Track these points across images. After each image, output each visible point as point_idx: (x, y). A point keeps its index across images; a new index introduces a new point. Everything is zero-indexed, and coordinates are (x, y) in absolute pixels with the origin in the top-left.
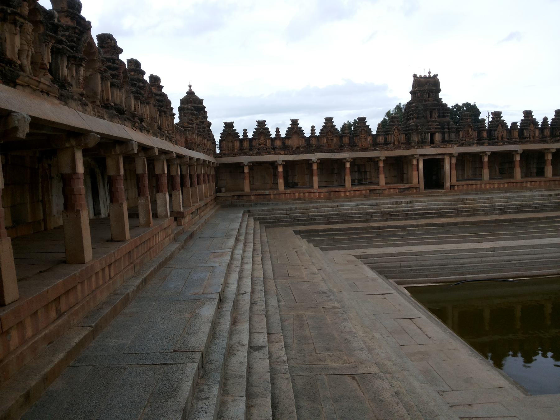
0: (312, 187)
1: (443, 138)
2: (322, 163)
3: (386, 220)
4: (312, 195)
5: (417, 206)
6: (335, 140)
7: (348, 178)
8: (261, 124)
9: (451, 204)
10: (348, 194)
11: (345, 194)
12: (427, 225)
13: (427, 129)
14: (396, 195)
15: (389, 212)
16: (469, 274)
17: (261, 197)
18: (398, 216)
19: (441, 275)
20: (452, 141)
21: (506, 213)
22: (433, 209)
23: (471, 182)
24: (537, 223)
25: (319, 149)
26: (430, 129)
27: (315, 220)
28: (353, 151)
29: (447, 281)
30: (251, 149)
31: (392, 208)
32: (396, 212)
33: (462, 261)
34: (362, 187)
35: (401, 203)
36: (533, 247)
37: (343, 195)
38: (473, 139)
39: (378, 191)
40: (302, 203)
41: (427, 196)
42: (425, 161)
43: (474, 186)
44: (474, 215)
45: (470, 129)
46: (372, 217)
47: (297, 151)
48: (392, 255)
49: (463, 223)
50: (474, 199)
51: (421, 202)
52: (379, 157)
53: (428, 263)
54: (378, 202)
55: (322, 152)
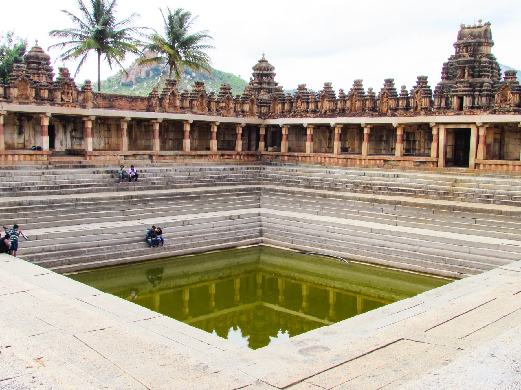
0: (333, 153)
1: (473, 103)
2: (346, 128)
3: (355, 191)
4: (332, 160)
5: (399, 181)
6: (357, 103)
7: (365, 145)
8: (302, 88)
9: (437, 184)
10: (363, 162)
11: (360, 162)
12: (369, 200)
13: (453, 91)
14: (410, 168)
15: (367, 184)
16: (327, 248)
17: (292, 158)
18: (371, 189)
19: (304, 243)
20: (481, 107)
21: (488, 202)
22: (411, 187)
23: (499, 162)
24: (489, 217)
25: (343, 113)
26: (456, 91)
27: (299, 182)
28: (372, 116)
29: (302, 249)
30: (290, 112)
31: (374, 180)
32: (374, 185)
33: (335, 235)
34: (376, 157)
35: (388, 176)
36: (424, 237)
37: (358, 162)
38: (510, 103)
39: (392, 163)
40: (320, 167)
41: (440, 173)
42: (448, 132)
43: (505, 167)
44: (449, 199)
45: (509, 92)
46: (347, 186)
47: (324, 115)
48: (289, 219)
49: (406, 204)
50: (470, 181)
51: (408, 177)
52: (391, 124)
53: (306, 231)
54: (365, 172)
55: (344, 116)
